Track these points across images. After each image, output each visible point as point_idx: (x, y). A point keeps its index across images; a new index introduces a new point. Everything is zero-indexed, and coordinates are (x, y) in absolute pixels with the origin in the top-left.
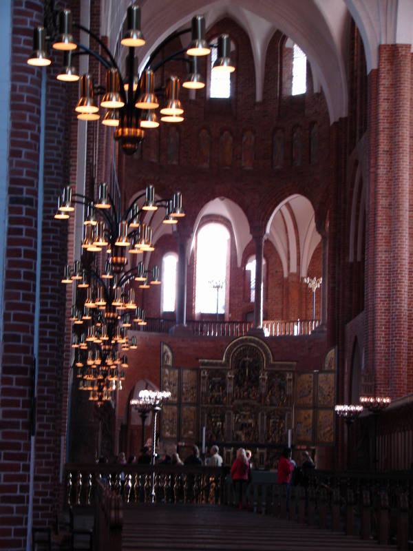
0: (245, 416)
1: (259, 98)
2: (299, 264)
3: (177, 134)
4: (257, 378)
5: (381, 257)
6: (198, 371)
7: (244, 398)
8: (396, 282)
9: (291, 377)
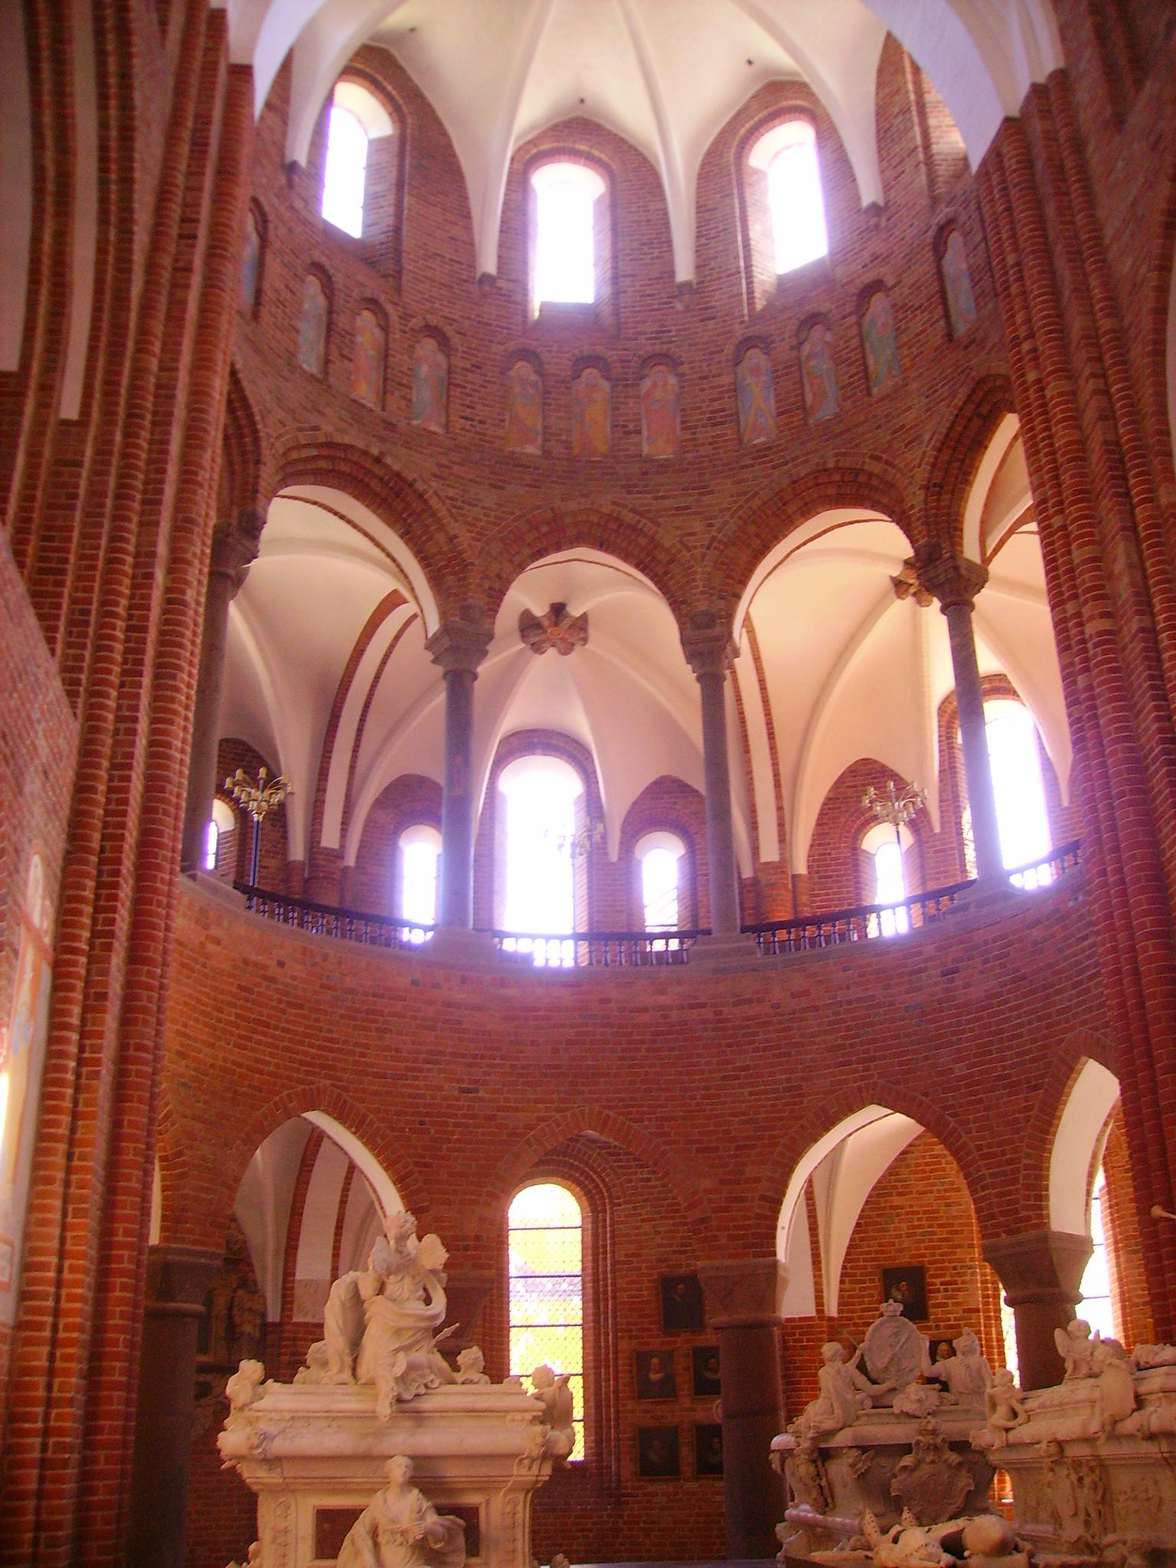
1: (684, 270)
2: (783, 839)
3: (441, 358)
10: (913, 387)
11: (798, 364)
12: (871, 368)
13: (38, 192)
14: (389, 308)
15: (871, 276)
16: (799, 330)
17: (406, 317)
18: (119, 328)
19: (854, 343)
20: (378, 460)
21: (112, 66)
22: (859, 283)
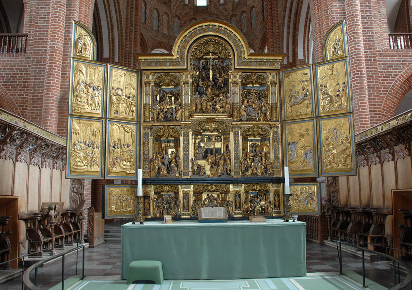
0: (209, 138)
4: (226, 82)
5: (336, 6)
6: (140, 73)
7: (207, 111)
8: (353, 25)
9: (275, 80)
10: (258, 28)
11: (241, 20)
12: (252, 23)
13: (109, 30)
14: (169, 13)
15: (252, 5)
16: (241, 13)
17: (172, 15)
18: (122, 45)
19: (249, 18)
20: (168, 43)
21: (117, 8)
22: (250, 7)
